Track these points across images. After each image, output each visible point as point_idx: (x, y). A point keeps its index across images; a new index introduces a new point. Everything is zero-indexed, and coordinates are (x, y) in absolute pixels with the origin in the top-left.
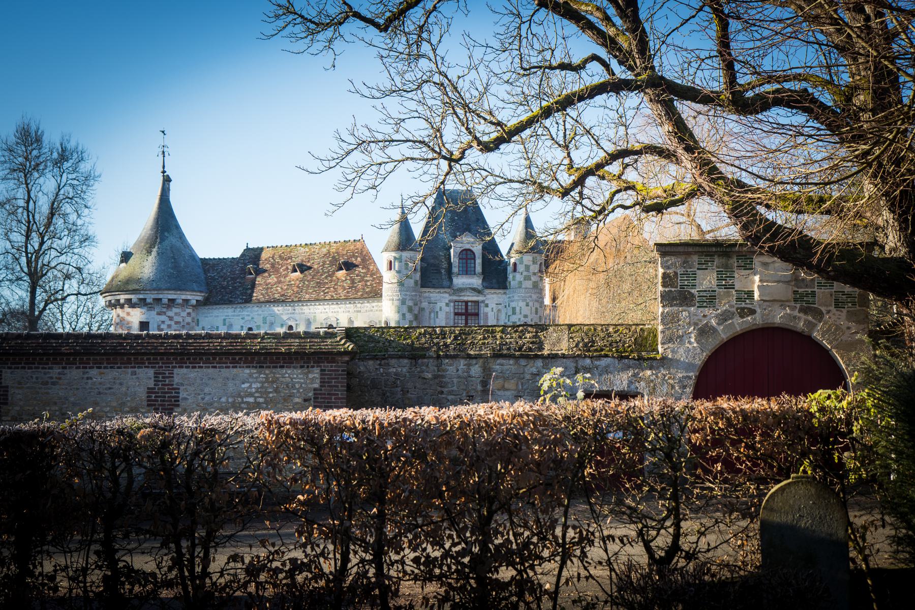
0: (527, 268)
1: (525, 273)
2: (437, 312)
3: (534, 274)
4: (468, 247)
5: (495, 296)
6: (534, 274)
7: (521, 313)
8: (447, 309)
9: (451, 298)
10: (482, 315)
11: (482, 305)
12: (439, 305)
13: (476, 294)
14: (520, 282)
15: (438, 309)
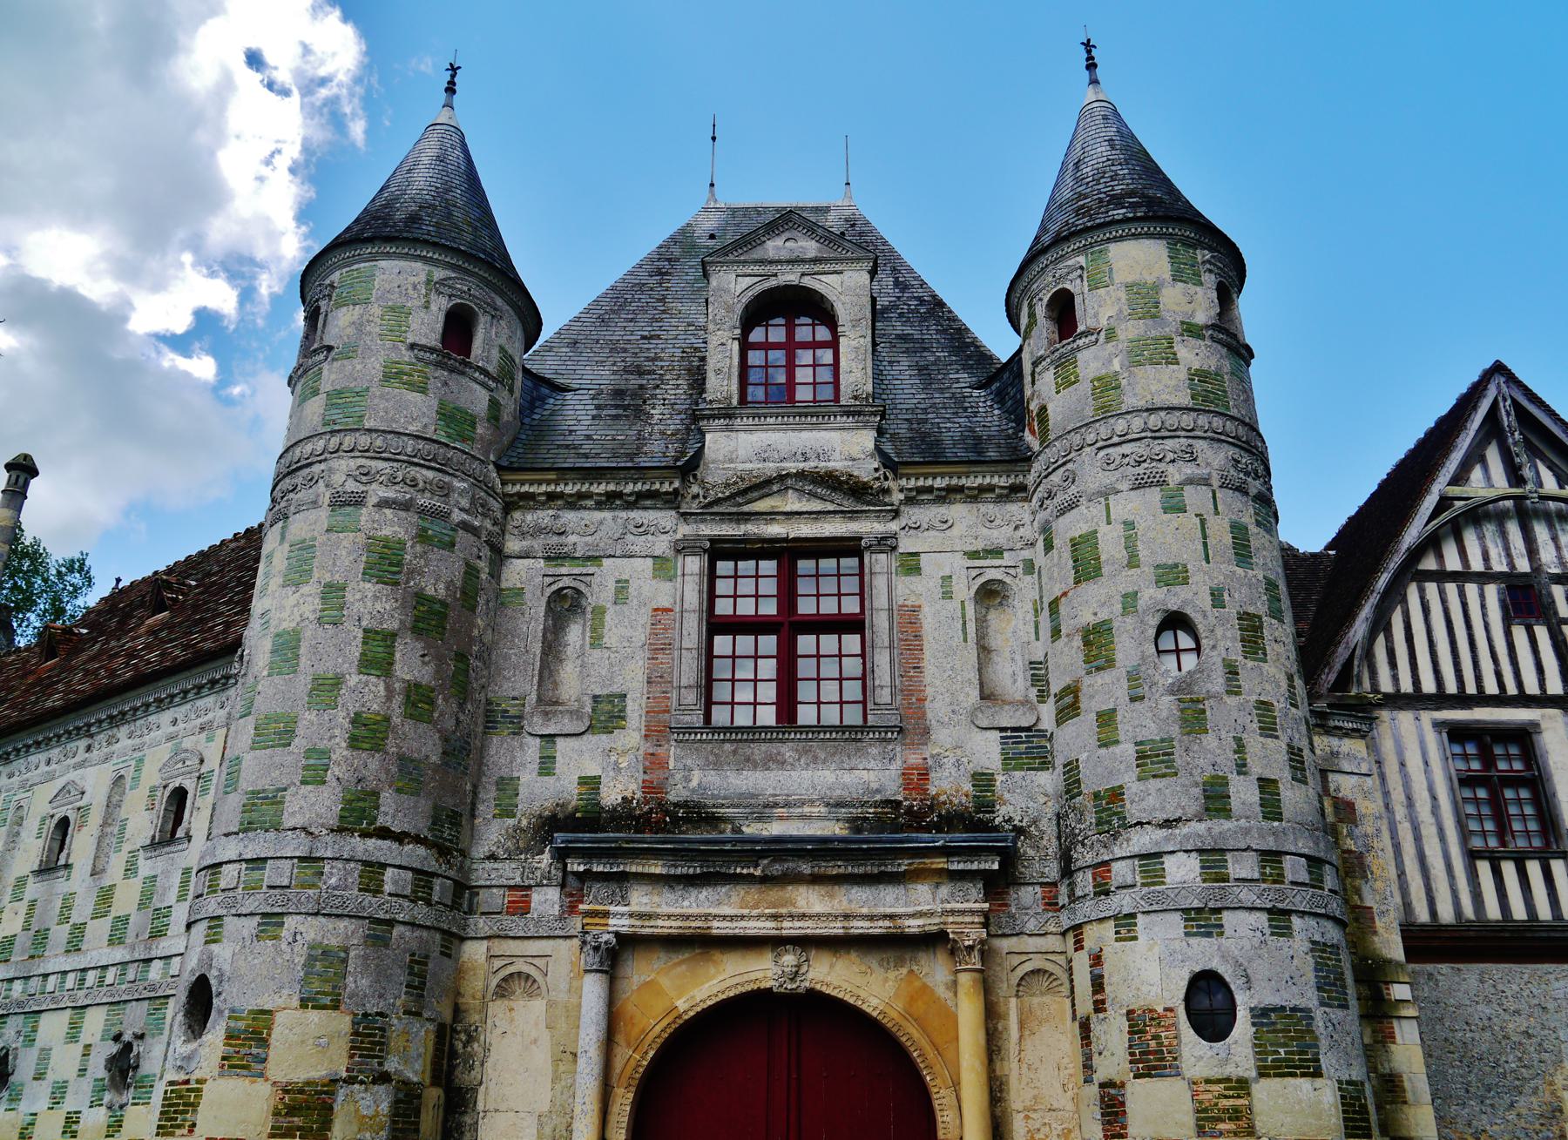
0: (1145, 301)
1: (1130, 330)
2: (600, 612)
3: (1191, 330)
4: (790, 277)
5: (958, 512)
6: (1191, 330)
7: (1133, 562)
8: (663, 594)
9: (685, 530)
10: (880, 623)
11: (879, 562)
12: (611, 569)
13: (848, 504)
14: (1106, 385)
15: (600, 592)
